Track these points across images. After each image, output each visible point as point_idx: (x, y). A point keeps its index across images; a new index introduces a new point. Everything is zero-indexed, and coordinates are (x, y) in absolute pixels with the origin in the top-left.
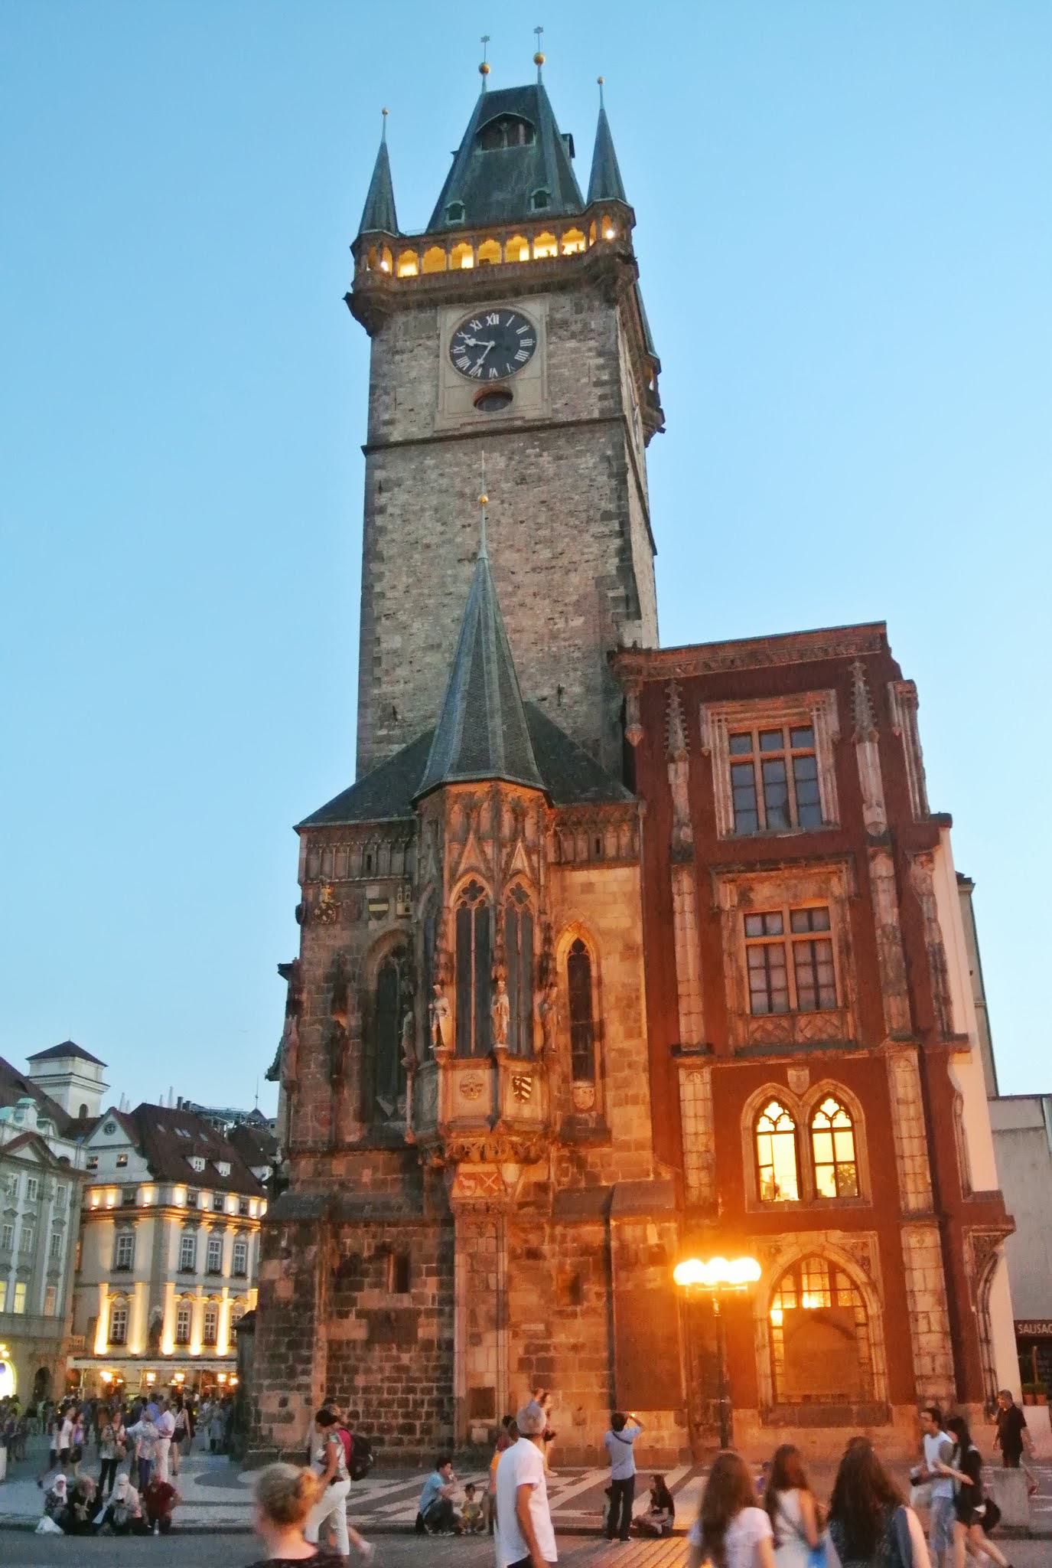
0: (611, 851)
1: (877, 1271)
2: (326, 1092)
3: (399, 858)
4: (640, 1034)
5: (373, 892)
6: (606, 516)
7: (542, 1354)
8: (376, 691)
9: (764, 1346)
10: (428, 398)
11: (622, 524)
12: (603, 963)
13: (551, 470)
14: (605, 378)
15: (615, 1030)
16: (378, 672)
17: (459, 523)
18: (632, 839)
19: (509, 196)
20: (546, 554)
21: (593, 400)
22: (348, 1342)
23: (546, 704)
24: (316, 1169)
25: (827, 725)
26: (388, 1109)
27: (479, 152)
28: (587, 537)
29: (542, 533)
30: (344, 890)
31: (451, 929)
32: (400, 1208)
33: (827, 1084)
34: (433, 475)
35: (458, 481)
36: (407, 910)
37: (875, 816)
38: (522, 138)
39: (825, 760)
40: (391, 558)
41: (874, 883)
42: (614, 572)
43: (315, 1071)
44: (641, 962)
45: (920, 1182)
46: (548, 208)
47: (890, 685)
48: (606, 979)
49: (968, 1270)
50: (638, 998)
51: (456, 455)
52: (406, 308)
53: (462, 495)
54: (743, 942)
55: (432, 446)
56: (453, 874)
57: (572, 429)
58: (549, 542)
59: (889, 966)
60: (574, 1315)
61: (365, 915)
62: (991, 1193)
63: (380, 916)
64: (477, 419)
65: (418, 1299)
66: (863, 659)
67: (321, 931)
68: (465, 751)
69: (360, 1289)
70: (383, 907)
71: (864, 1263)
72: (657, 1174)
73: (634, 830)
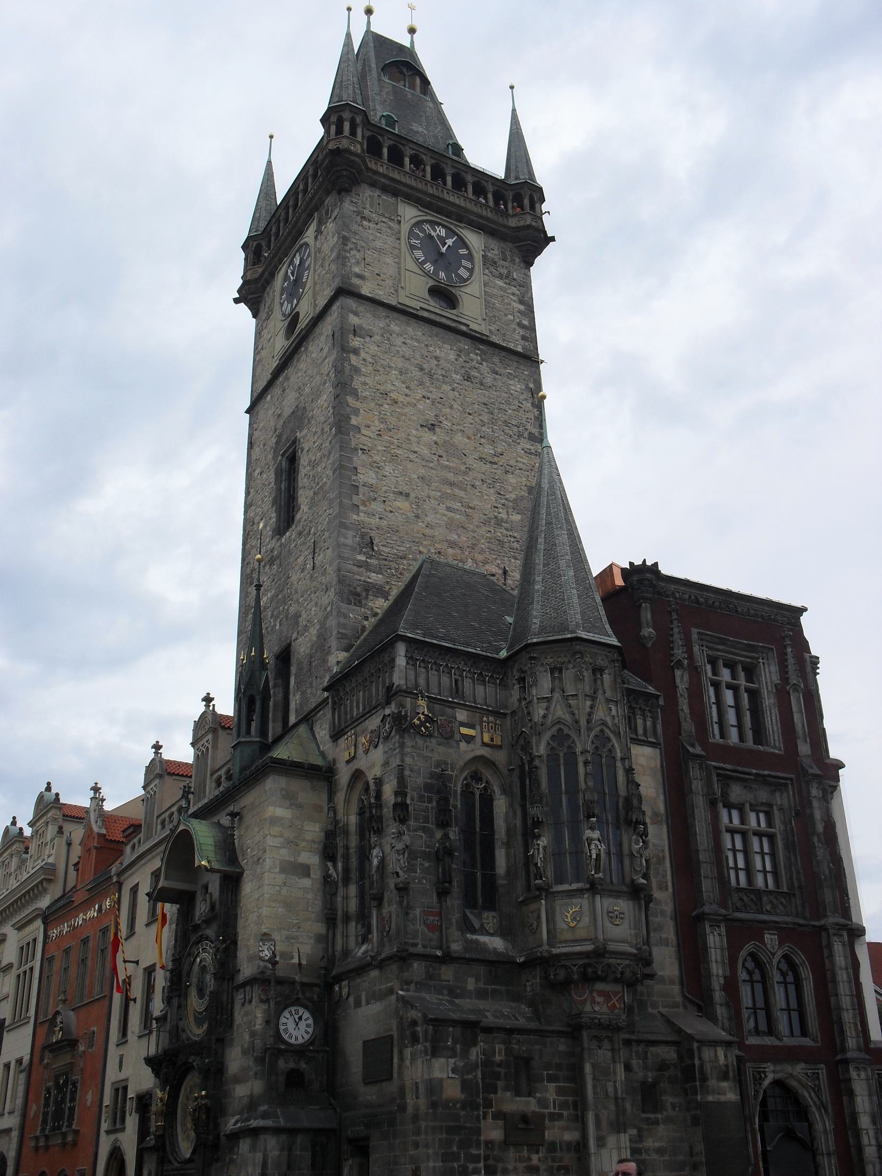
3: (480, 689)
4: (667, 890)
5: (462, 715)
8: (355, 517)
10: (392, 271)
13: (489, 380)
14: (526, 323)
16: (356, 500)
17: (420, 392)
26: (476, 924)
28: (519, 448)
30: (437, 707)
35: (418, 356)
36: (492, 740)
50: (664, 858)
51: (415, 331)
52: (373, 185)
53: (422, 369)
55: (396, 315)
57: (504, 354)
60: (656, 1122)
61: (457, 737)
63: (469, 739)
64: (432, 309)
67: (420, 741)
68: (583, 613)
70: (471, 732)
72: (685, 1007)
73: (654, 719)
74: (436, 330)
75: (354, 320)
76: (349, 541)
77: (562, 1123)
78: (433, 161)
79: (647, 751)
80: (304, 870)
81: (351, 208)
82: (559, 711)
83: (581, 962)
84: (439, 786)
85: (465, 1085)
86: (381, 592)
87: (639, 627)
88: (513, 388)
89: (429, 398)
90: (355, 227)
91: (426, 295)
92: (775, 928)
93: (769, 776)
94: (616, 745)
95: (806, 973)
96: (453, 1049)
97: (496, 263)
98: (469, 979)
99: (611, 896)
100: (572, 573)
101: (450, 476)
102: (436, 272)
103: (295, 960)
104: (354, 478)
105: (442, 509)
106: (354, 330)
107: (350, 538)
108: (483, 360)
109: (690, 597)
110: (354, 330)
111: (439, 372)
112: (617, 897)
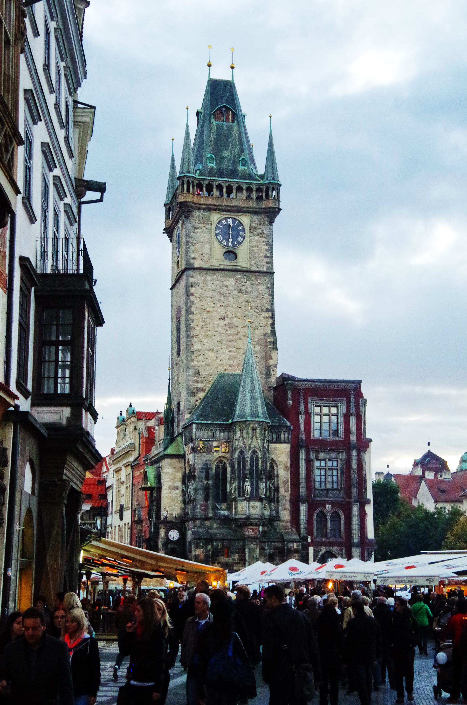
0: (282, 439)
2: (203, 502)
3: (222, 434)
4: (288, 492)
5: (215, 444)
6: (268, 310)
8: (193, 364)
10: (207, 251)
12: (279, 471)
13: (249, 290)
14: (268, 255)
15: (282, 490)
16: (193, 357)
21: (264, 263)
26: (219, 507)
27: (214, 122)
28: (261, 317)
29: (247, 313)
30: (206, 443)
31: (248, 463)
33: (335, 509)
34: (210, 284)
37: (353, 438)
38: (231, 121)
39: (341, 419)
40: (196, 314)
42: (270, 332)
44: (289, 472)
47: (361, 399)
51: (218, 276)
52: (199, 209)
53: (220, 293)
55: (209, 272)
56: (249, 447)
57: (257, 274)
61: (213, 451)
63: (217, 451)
64: (225, 263)
65: (234, 559)
66: (354, 391)
67: (200, 454)
68: (251, 410)
69: (218, 556)
72: (292, 529)
73: (289, 433)
75: (191, 280)
76: (191, 374)
77: (240, 565)
78: (227, 184)
80: (177, 488)
81: (190, 225)
82: (241, 444)
83: (243, 521)
84: (206, 468)
86: (202, 390)
87: (287, 400)
88: (260, 289)
90: (192, 234)
91: (223, 258)
92: (330, 503)
93: (335, 449)
95: (342, 517)
97: (255, 228)
100: (250, 395)
101: (231, 338)
103: (174, 516)
104: (192, 348)
105: (227, 352)
106: (192, 285)
107: (191, 372)
108: (247, 280)
110: (192, 285)
111: (228, 292)
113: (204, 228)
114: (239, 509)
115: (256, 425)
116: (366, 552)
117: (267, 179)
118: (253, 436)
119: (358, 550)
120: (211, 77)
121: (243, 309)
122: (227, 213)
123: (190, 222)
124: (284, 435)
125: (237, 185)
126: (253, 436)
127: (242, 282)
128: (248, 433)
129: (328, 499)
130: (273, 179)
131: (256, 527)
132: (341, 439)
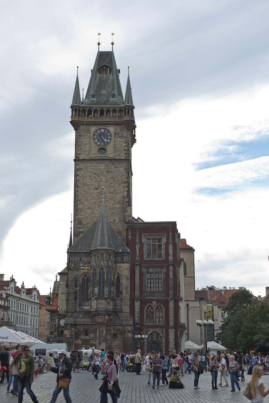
0: (125, 260)
1: (164, 335)
3: (86, 259)
4: (128, 294)
5: (81, 265)
6: (125, 182)
7: (110, 346)
8: (77, 217)
9: (146, 346)
10: (88, 149)
11: (128, 184)
12: (123, 280)
13: (114, 171)
14: (126, 149)
15: (124, 293)
17: (95, 180)
18: (129, 259)
19: (105, 92)
20: (112, 190)
21: (124, 154)
22: (78, 344)
23: (111, 223)
24: (71, 314)
25: (164, 240)
27: (98, 75)
28: (121, 186)
32: (87, 322)
33: (159, 304)
36: (88, 269)
37: (171, 258)
38: (108, 73)
39: (163, 247)
41: (170, 270)
42: (126, 196)
43: (72, 297)
45: (172, 321)
46: (115, 99)
48: (123, 283)
49: (179, 335)
50: (128, 287)
51: (94, 164)
52: (83, 125)
53: (95, 174)
54: (147, 278)
55: (89, 161)
56: (98, 266)
57: (119, 161)
58: (113, 187)
59: (171, 285)
60: (116, 340)
61: (80, 269)
62: (184, 323)
63: (83, 269)
64: (99, 156)
65: (90, 337)
67: (72, 272)
70: (84, 268)
71: (163, 334)
72: (130, 318)
74: (100, 161)
78: (101, 109)
79: (127, 264)
83: (94, 312)
85: (71, 335)
86: (82, 232)
88: (121, 170)
89: (97, 181)
92: (156, 300)
93: (159, 266)
94: (105, 270)
96: (69, 329)
98: (80, 315)
99: (100, 300)
102: (100, 145)
103: (64, 310)
106: (78, 170)
109: (142, 226)
110: (78, 170)
112: (102, 300)
113: (86, 136)
114: (93, 305)
115: (104, 252)
116: (179, 332)
117: (125, 104)
118: (101, 259)
119: (173, 331)
120: (100, 51)
121: (110, 183)
122: (100, 126)
123: (78, 132)
124: (126, 258)
125: (107, 109)
126: (101, 259)
127: (109, 166)
128: (98, 257)
129: (154, 298)
130: (128, 103)
131: (103, 316)
132: (163, 259)
